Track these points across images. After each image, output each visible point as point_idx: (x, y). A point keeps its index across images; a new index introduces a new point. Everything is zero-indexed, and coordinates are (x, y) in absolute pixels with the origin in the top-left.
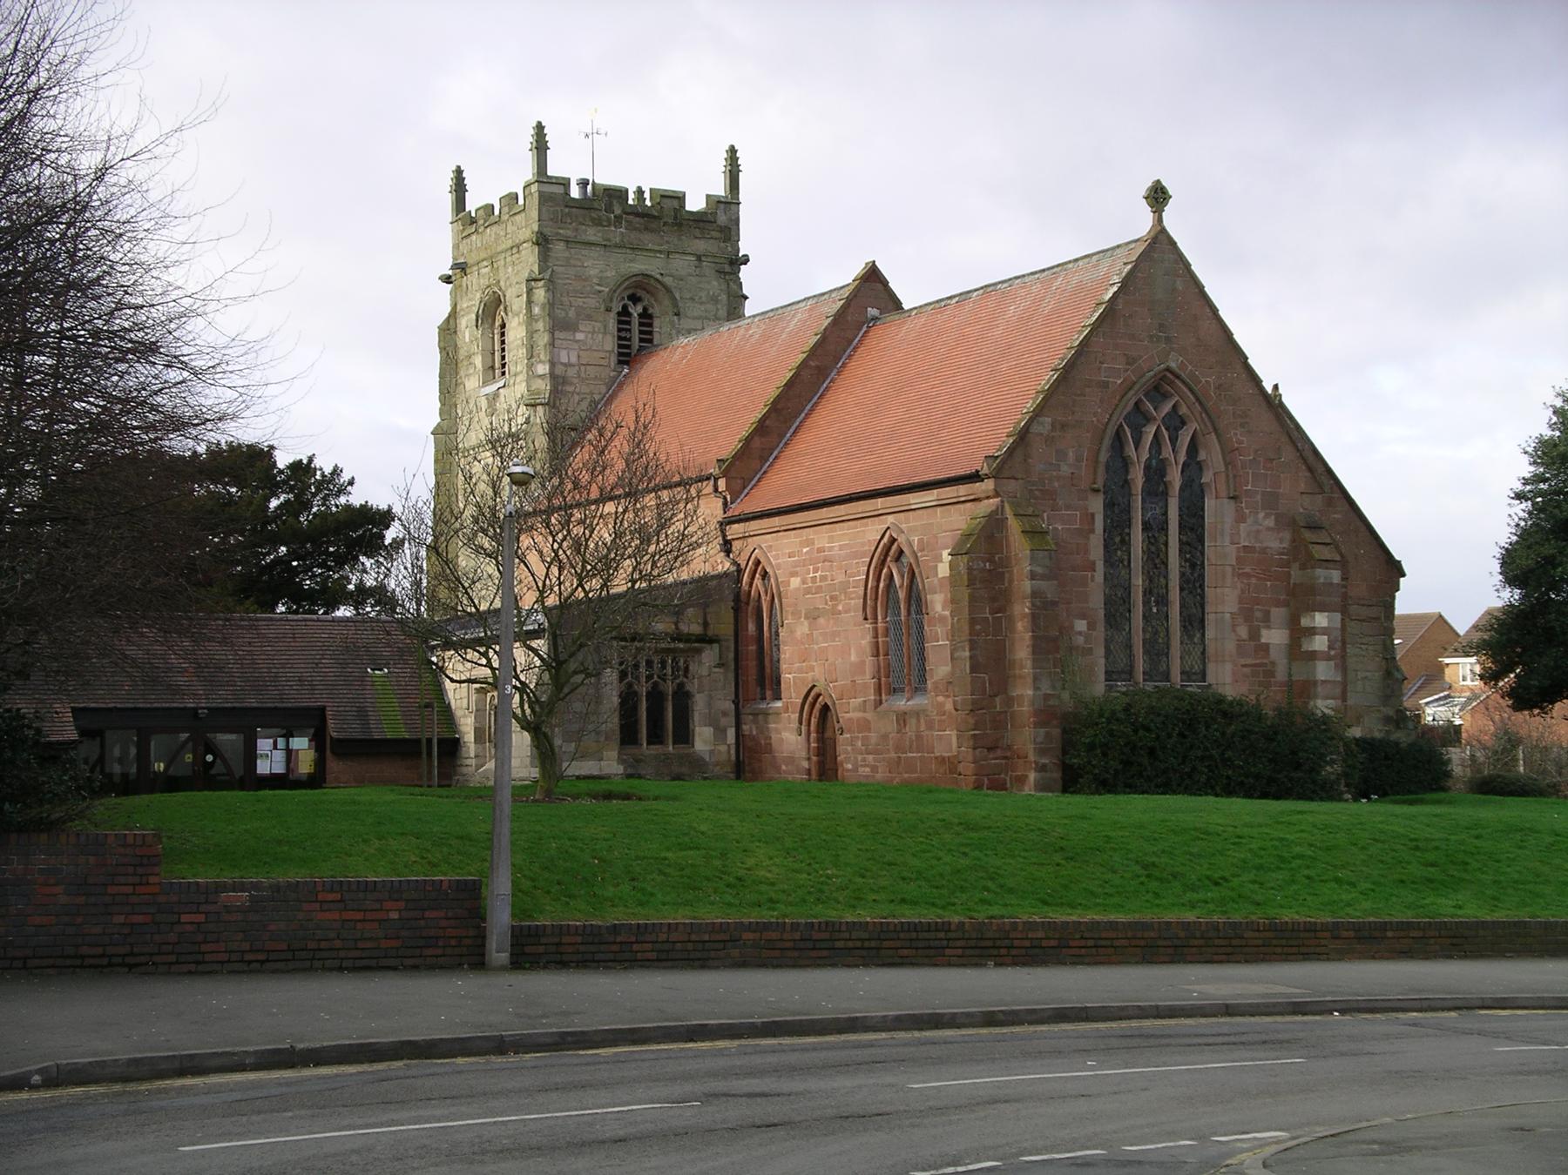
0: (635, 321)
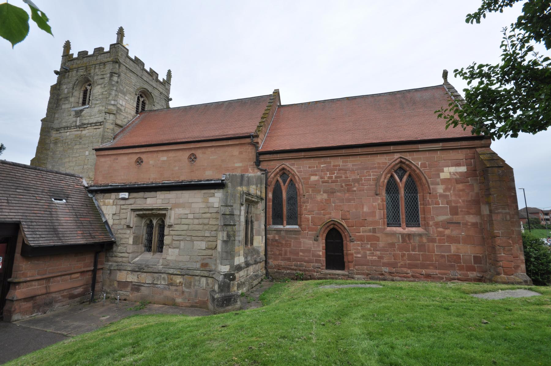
0: (141, 103)
